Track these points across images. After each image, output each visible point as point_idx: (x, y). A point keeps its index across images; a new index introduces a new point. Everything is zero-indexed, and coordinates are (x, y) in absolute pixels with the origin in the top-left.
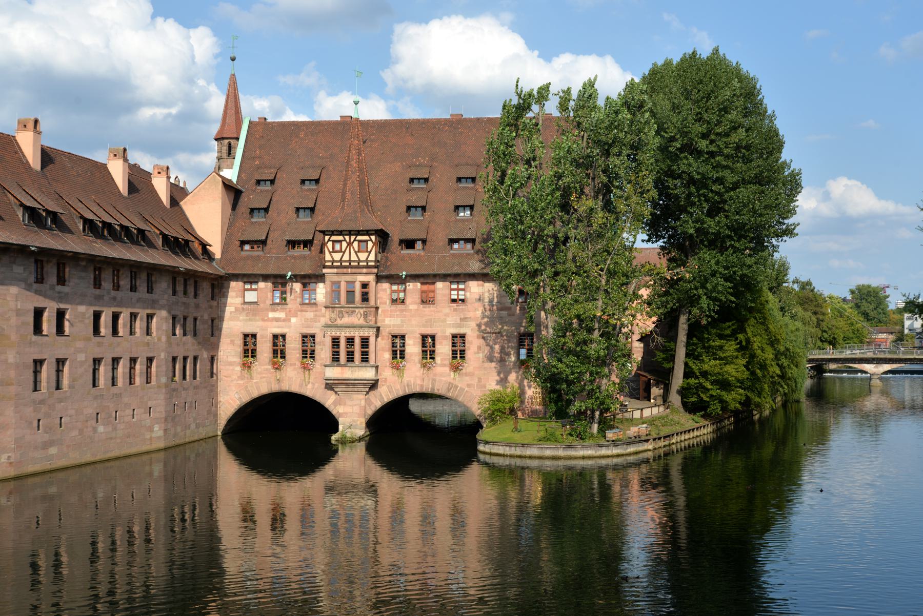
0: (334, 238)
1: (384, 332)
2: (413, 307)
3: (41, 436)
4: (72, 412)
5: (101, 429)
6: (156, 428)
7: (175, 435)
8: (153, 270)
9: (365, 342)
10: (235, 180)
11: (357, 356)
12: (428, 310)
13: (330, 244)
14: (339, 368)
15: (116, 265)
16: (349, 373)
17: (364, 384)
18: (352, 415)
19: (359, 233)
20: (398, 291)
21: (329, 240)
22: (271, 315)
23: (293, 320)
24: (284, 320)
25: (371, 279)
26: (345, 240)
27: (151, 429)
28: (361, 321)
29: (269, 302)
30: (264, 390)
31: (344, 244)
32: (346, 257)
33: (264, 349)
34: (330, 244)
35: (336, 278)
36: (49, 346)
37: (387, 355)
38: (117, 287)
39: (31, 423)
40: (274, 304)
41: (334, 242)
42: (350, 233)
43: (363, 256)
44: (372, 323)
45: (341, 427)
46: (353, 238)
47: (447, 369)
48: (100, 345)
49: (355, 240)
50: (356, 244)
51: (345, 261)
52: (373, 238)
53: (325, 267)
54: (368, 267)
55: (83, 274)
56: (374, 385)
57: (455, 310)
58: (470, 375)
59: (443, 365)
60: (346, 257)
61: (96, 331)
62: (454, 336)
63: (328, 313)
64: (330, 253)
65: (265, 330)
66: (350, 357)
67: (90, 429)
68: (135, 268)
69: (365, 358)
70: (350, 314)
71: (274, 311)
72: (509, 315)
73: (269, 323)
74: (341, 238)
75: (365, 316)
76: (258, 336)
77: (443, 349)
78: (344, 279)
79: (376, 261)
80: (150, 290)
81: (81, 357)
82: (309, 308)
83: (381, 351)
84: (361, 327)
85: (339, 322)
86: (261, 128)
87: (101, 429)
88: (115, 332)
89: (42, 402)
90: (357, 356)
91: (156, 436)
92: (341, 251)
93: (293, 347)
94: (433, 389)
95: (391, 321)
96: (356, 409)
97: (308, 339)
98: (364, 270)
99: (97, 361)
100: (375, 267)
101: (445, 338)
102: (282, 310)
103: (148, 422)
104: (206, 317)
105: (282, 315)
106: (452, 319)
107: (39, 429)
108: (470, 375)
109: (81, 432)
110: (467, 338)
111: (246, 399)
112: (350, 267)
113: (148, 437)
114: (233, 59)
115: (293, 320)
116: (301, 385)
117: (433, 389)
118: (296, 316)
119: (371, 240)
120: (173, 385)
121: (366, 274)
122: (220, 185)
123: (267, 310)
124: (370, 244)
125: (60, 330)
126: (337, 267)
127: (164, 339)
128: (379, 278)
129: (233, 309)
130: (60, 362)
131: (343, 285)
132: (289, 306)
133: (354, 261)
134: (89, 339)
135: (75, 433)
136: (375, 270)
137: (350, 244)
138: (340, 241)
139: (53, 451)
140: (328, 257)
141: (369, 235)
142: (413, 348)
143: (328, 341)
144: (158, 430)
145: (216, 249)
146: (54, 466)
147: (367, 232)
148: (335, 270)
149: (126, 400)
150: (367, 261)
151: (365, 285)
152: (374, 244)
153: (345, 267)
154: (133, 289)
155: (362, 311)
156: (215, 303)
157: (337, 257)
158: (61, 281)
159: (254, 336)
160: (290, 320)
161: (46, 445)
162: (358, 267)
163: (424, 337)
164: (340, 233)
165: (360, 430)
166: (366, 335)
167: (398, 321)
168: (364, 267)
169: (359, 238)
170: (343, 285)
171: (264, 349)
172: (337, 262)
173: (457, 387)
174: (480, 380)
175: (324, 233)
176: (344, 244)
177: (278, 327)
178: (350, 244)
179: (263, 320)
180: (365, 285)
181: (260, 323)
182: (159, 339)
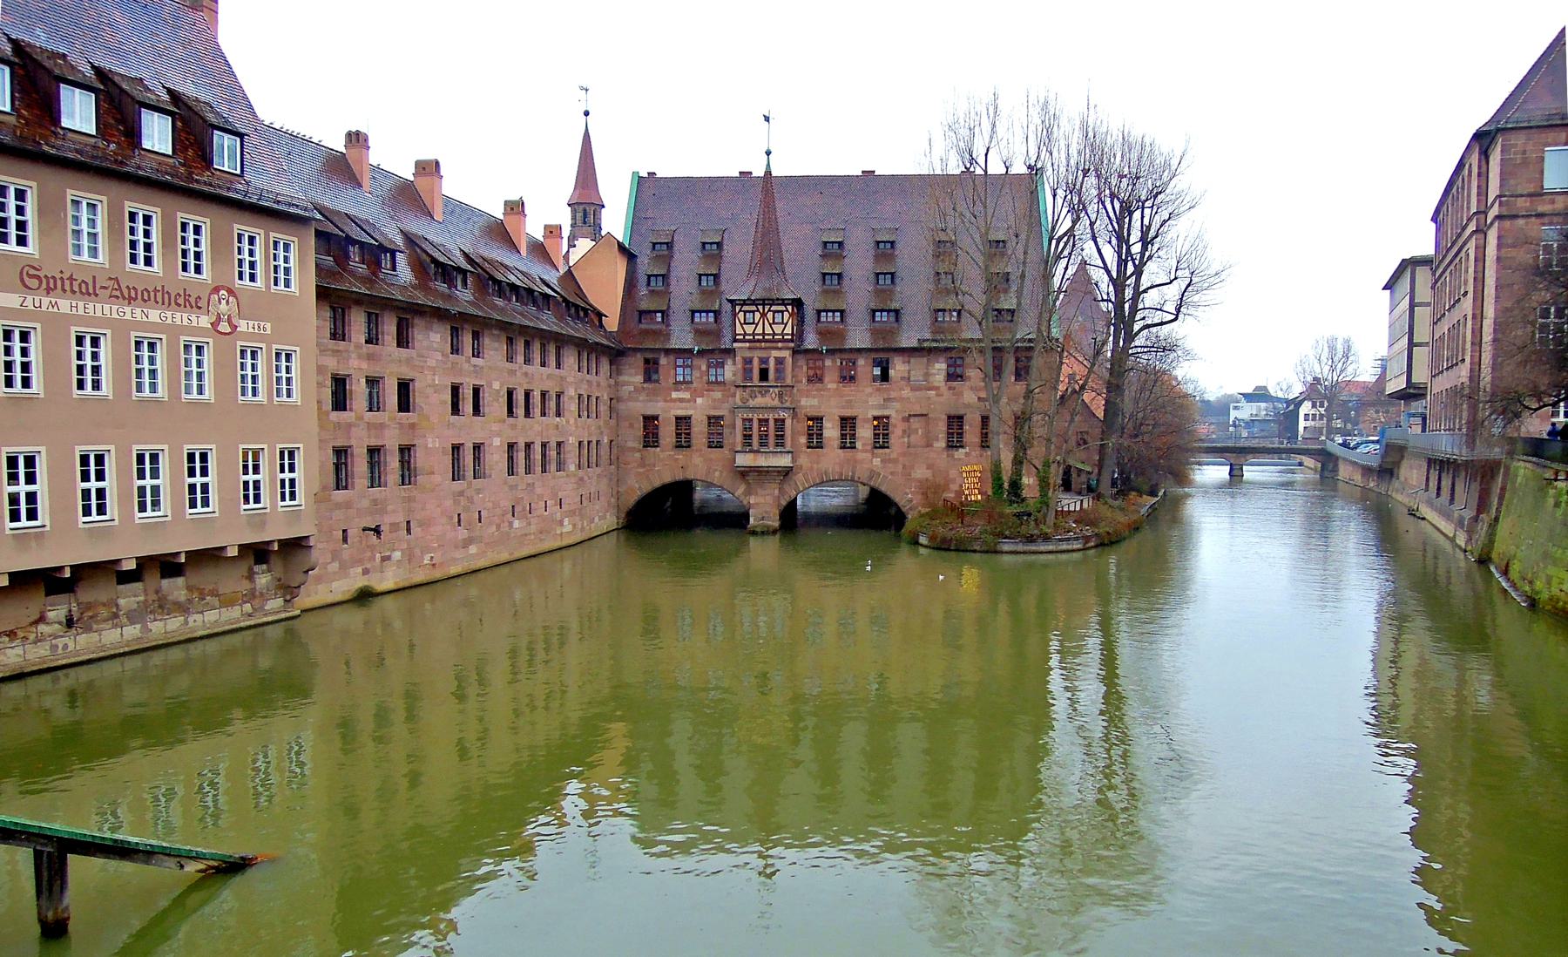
0: (746, 308)
1: (802, 417)
2: (834, 386)
3: (462, 533)
5: (516, 524)
7: (583, 529)
8: (561, 341)
9: (780, 423)
11: (772, 440)
12: (848, 389)
13: (741, 315)
14: (751, 456)
15: (530, 335)
16: (762, 461)
18: (763, 506)
19: (773, 302)
22: (674, 395)
23: (699, 400)
25: (786, 354)
27: (561, 523)
28: (776, 403)
30: (668, 479)
33: (667, 433)
34: (741, 315)
35: (748, 354)
36: (468, 429)
37: (803, 440)
38: (527, 361)
39: (451, 518)
40: (677, 383)
42: (764, 302)
48: (513, 427)
50: (770, 315)
53: (736, 341)
54: (783, 341)
55: (496, 345)
56: (786, 472)
58: (895, 461)
60: (759, 330)
61: (510, 412)
62: (875, 418)
63: (739, 393)
65: (668, 408)
66: (763, 441)
68: (546, 337)
69: (780, 440)
70: (764, 392)
75: (781, 395)
77: (865, 433)
78: (756, 355)
80: (558, 366)
81: (497, 442)
82: (716, 387)
83: (796, 433)
84: (774, 408)
85: (752, 403)
86: (648, 188)
88: (527, 414)
89: (461, 493)
90: (772, 440)
91: (568, 530)
93: (699, 429)
95: (809, 403)
96: (769, 499)
97: (714, 421)
99: (511, 446)
101: (866, 420)
102: (687, 390)
103: (558, 517)
104: (606, 397)
105: (686, 395)
106: (876, 400)
108: (895, 461)
109: (498, 527)
110: (892, 421)
111: (647, 488)
115: (699, 400)
116: (708, 472)
120: (581, 473)
123: (670, 390)
124: (786, 315)
125: (477, 410)
127: (572, 421)
128: (795, 352)
130: (477, 448)
131: (756, 362)
137: (764, 315)
139: (473, 549)
140: (739, 330)
142: (831, 431)
143: (739, 423)
144: (567, 527)
145: (612, 323)
146: (474, 567)
147: (783, 302)
149: (539, 491)
150: (782, 334)
151: (780, 361)
154: (543, 364)
156: (612, 382)
158: (477, 354)
159: (656, 418)
161: (467, 543)
163: (844, 420)
164: (754, 303)
165: (777, 524)
167: (815, 402)
170: (756, 362)
171: (667, 433)
175: (731, 301)
176: (757, 315)
178: (764, 315)
180: (780, 361)
181: (661, 404)
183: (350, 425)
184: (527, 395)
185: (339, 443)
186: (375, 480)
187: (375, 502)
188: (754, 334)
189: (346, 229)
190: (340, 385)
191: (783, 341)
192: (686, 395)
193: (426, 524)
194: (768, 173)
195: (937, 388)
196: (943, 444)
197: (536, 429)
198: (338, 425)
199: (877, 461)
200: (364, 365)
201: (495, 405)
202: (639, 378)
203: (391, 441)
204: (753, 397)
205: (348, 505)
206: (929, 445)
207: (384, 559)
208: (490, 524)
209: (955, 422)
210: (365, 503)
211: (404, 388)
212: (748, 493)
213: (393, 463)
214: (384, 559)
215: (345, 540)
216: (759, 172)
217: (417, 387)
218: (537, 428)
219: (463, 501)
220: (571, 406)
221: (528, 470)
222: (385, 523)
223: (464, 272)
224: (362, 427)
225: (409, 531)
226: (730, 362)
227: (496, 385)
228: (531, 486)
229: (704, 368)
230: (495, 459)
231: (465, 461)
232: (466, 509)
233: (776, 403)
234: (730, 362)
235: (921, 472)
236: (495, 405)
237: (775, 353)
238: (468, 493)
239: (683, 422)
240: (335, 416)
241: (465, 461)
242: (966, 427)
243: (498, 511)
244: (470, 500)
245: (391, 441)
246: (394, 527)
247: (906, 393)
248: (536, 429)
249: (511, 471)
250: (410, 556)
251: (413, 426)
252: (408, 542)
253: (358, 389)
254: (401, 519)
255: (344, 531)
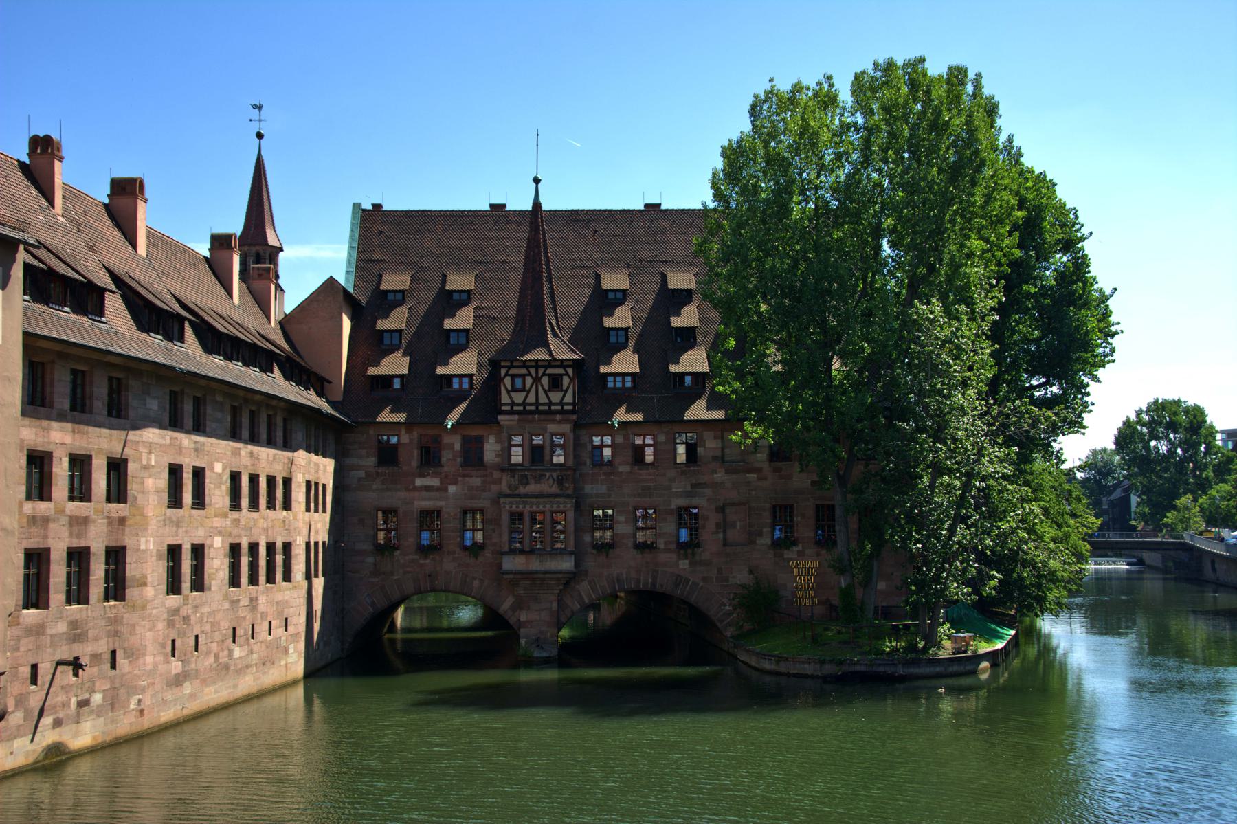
3: (176, 666)
4: (208, 628)
5: (238, 652)
6: (291, 651)
10: (351, 290)
13: (508, 381)
17: (558, 579)
20: (602, 446)
21: (507, 374)
22: (419, 482)
23: (452, 489)
24: (438, 489)
26: (530, 374)
27: (286, 651)
28: (554, 489)
29: (415, 463)
31: (529, 380)
32: (531, 399)
34: (508, 381)
41: (513, 376)
43: (556, 397)
44: (570, 492)
45: (523, 642)
46: (541, 371)
47: (674, 556)
49: (544, 374)
51: (531, 404)
52: (570, 371)
54: (562, 412)
55: (219, 415)
57: (683, 473)
59: (668, 551)
60: (531, 399)
64: (508, 392)
67: (226, 653)
71: (422, 475)
72: (759, 479)
73: (416, 494)
74: (524, 371)
75: (560, 482)
76: (400, 512)
79: (573, 404)
81: (218, 542)
84: (555, 496)
85: (522, 490)
87: (238, 652)
89: (176, 611)
92: (523, 390)
94: (654, 584)
98: (558, 417)
100: (573, 412)
102: (435, 474)
105: (435, 482)
107: (173, 655)
109: (217, 657)
112: (537, 412)
113: (283, 663)
114: (260, 136)
115: (452, 489)
117: (654, 584)
118: (455, 483)
119: (567, 374)
121: (560, 422)
122: (341, 297)
126: (518, 413)
129: (362, 474)
132: (446, 469)
133: (543, 404)
134: (226, 516)
135: (211, 659)
136: (574, 417)
137: (537, 380)
138: (523, 376)
139: (187, 688)
140: (505, 399)
141: (565, 367)
148: (517, 417)
150: (561, 403)
152: (571, 379)
153: (531, 412)
155: (555, 474)
157: (519, 397)
160: (446, 490)
162: (549, 412)
166: (562, 507)
168: (557, 412)
169: (550, 371)
172: (518, 405)
173: (687, 581)
174: (720, 571)
176: (529, 380)
177: (430, 499)
178: (537, 380)
179: (407, 489)
181: (403, 494)
182: (295, 517)
183: (46, 520)
184: (254, 479)
185: (34, 543)
186: (78, 593)
187: (74, 624)
188: (524, 404)
189: (46, 260)
190: (38, 462)
191: (562, 412)
192: (435, 482)
193: (133, 654)
194: (537, 204)
195: (758, 470)
196: (769, 542)
197: (263, 525)
198: (33, 520)
199: (684, 564)
200: (68, 439)
201: (218, 494)
202: (371, 461)
203: (97, 542)
204: (524, 481)
205: (38, 630)
206: (752, 542)
207: (84, 704)
208: (208, 652)
209: (783, 513)
210: (62, 627)
211: (117, 468)
212: (519, 606)
213: (98, 571)
214: (84, 704)
215: (34, 680)
216: (520, 202)
217: (131, 467)
218: (262, 524)
219: (179, 624)
220: (299, 495)
221: (253, 580)
222: (84, 651)
223: (181, 320)
224: (63, 523)
225: (113, 666)
226: (492, 439)
227: (218, 467)
228: (253, 600)
229: (458, 447)
230: (217, 565)
231: (186, 570)
232: (182, 634)
233: (554, 489)
234: (492, 439)
235: (741, 576)
236: (218, 494)
237: (552, 427)
238: (187, 610)
239: (429, 517)
240: (28, 507)
241: (186, 570)
242: (797, 519)
243: (217, 636)
244: (186, 619)
245: (97, 542)
246: (96, 657)
247: (720, 476)
248: (263, 525)
249: (234, 581)
250: (113, 703)
251: (122, 521)
252: (112, 679)
253: (61, 470)
254: (103, 647)
255: (34, 667)
